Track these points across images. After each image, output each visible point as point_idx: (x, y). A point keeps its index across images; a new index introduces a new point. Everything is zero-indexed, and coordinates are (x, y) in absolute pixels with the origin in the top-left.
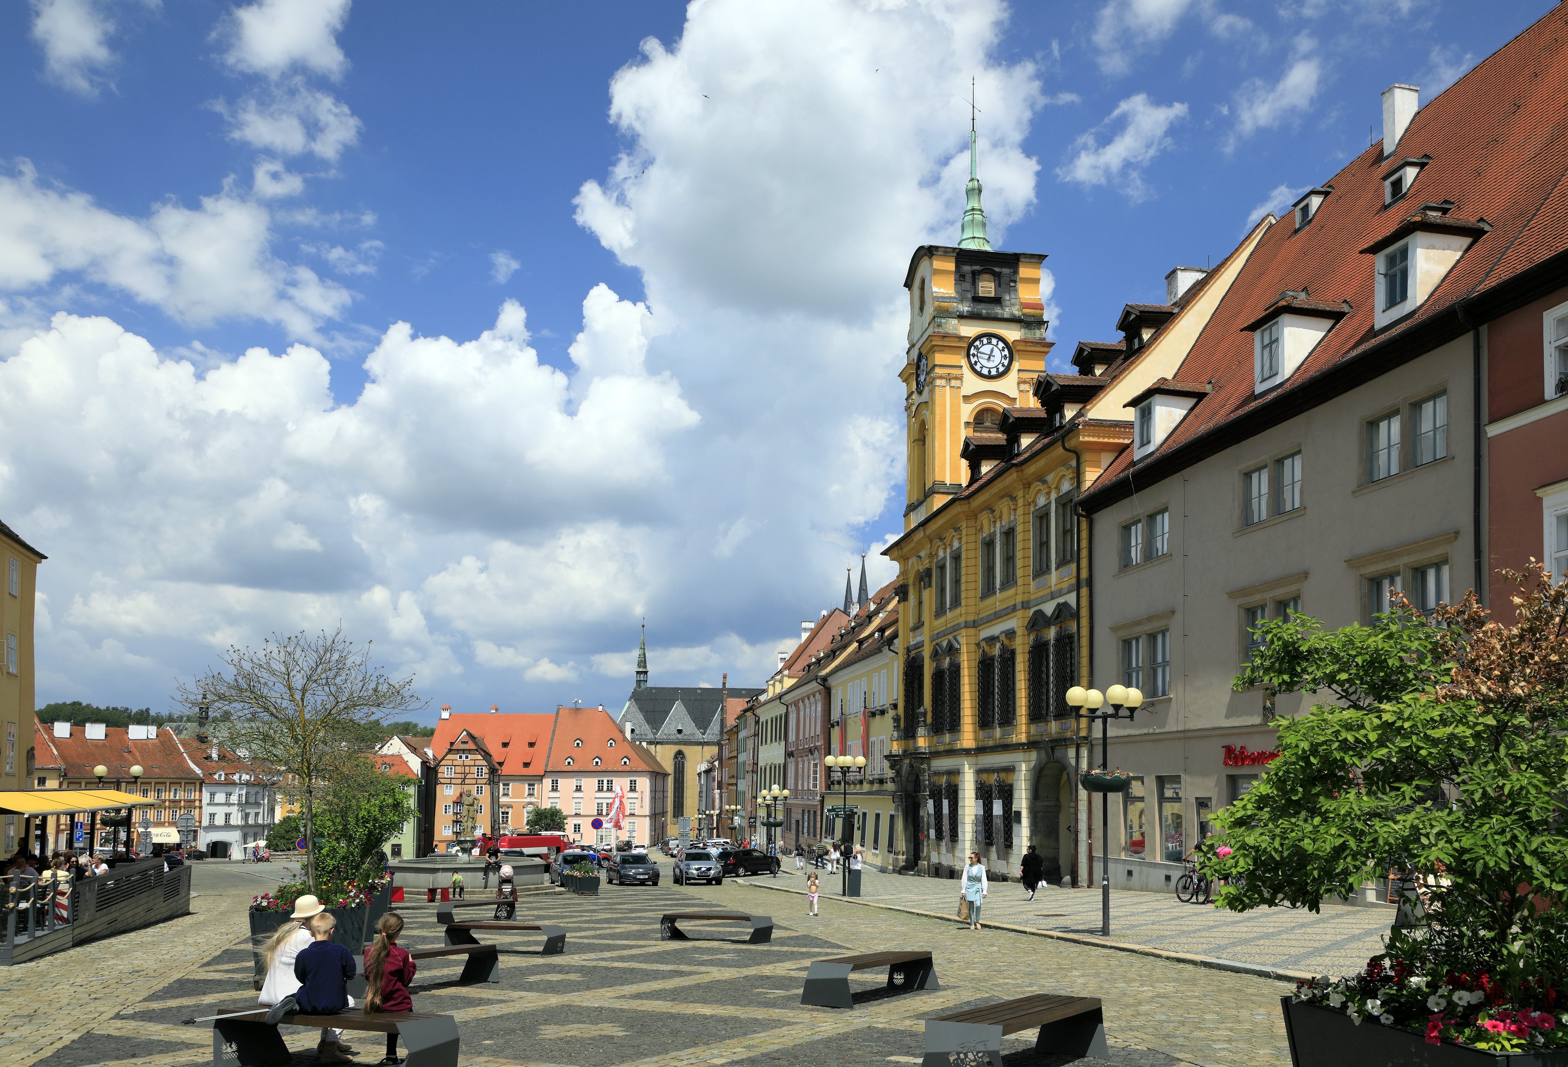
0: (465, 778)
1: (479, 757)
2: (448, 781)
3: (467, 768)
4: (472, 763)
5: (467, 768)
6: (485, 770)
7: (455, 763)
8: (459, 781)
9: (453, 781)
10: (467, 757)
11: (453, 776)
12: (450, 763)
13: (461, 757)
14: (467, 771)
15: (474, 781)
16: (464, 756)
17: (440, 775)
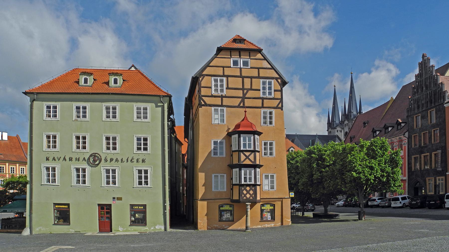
0: (244, 98)
1: (265, 64)
2: (218, 101)
3: (247, 81)
4: (255, 73)
5: (247, 81)
6: (275, 85)
7: (228, 72)
8: (237, 102)
9: (226, 101)
10: (245, 64)
11: (225, 93)
12: (220, 71)
13: (235, 63)
14: (247, 86)
15: (258, 103)
16: (241, 62)
17: (204, 92)
